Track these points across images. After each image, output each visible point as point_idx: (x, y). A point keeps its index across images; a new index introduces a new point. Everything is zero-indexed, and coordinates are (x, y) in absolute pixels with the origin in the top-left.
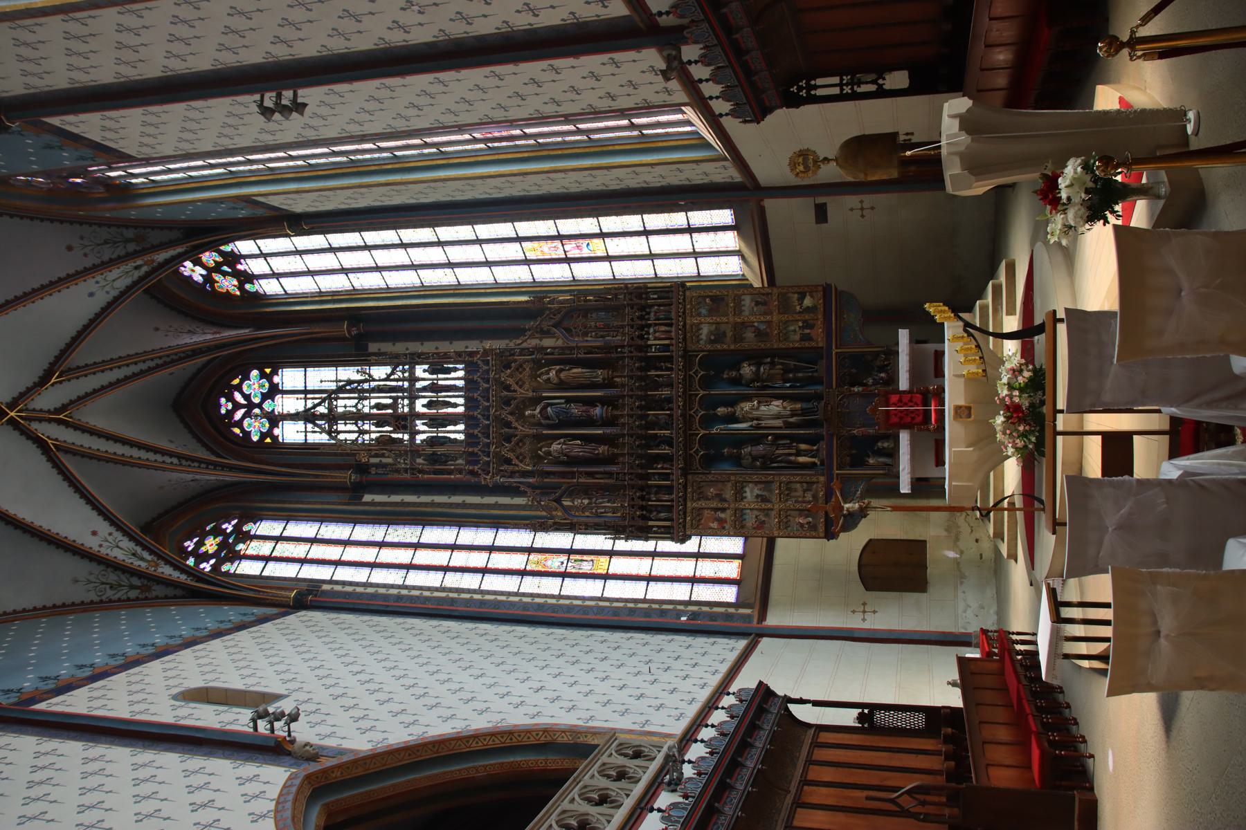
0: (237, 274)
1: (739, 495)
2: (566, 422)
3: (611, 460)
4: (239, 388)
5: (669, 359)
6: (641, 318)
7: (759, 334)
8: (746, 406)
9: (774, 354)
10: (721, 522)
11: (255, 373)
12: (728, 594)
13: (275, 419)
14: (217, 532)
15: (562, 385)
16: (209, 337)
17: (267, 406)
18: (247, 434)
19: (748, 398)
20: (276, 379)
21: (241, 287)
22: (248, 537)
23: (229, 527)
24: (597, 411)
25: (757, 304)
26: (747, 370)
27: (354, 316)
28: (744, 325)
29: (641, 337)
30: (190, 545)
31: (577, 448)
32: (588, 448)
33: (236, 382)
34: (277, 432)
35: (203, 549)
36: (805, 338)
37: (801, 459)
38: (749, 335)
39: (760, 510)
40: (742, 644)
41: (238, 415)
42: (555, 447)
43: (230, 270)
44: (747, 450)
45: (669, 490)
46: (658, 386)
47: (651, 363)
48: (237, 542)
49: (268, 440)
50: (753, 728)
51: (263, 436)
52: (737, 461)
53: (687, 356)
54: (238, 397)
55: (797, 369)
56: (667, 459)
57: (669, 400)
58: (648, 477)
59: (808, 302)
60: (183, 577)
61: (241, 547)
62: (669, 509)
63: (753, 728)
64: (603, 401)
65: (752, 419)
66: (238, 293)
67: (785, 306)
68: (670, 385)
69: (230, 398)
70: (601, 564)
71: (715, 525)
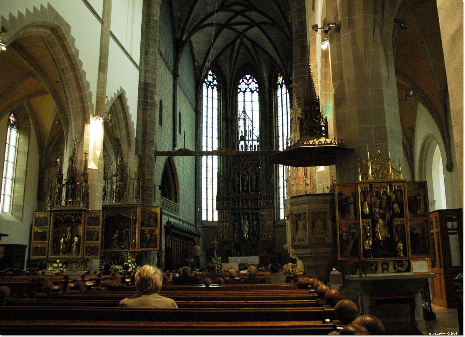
0: (282, 84)
1: (226, 222)
2: (243, 180)
3: (234, 191)
4: (253, 81)
5: (257, 205)
6: (267, 198)
7: (263, 226)
8: (247, 223)
9: (259, 229)
10: (221, 218)
11: (257, 86)
12: (204, 218)
13: (244, 92)
14: (214, 79)
15: (251, 180)
16: (265, 77)
17: (248, 90)
18: (240, 84)
19: (249, 223)
20: (255, 92)
21: (279, 84)
22: (213, 88)
23: (215, 82)
24: (245, 188)
25: (270, 225)
26: (255, 223)
27: (271, 117)
28: (265, 222)
29: (262, 198)
30: (210, 72)
31: (237, 183)
32: (237, 187)
33: (255, 80)
34: (241, 93)
35: (209, 76)
36: (262, 236)
37: (235, 235)
38: (263, 223)
39: (223, 227)
40: (194, 224)
41: (245, 81)
42: (237, 178)
43: (283, 82)
44: (237, 223)
45: (227, 205)
46: (251, 202)
47: (256, 200)
48: (211, 86)
49: (239, 90)
50: (180, 230)
51: (240, 89)
52: (235, 221)
53: (258, 209)
54: (251, 81)
55: (255, 234)
56: (235, 205)
57: (248, 205)
58: (230, 200)
59: (270, 236)
60: (202, 79)
61: (210, 87)
62: (223, 205)
63: (180, 230)
64: (248, 190)
65: (244, 224)
66: (278, 83)
67: (269, 231)
68: (252, 205)
69: (250, 78)
70: (210, 187)
71: (220, 216)
